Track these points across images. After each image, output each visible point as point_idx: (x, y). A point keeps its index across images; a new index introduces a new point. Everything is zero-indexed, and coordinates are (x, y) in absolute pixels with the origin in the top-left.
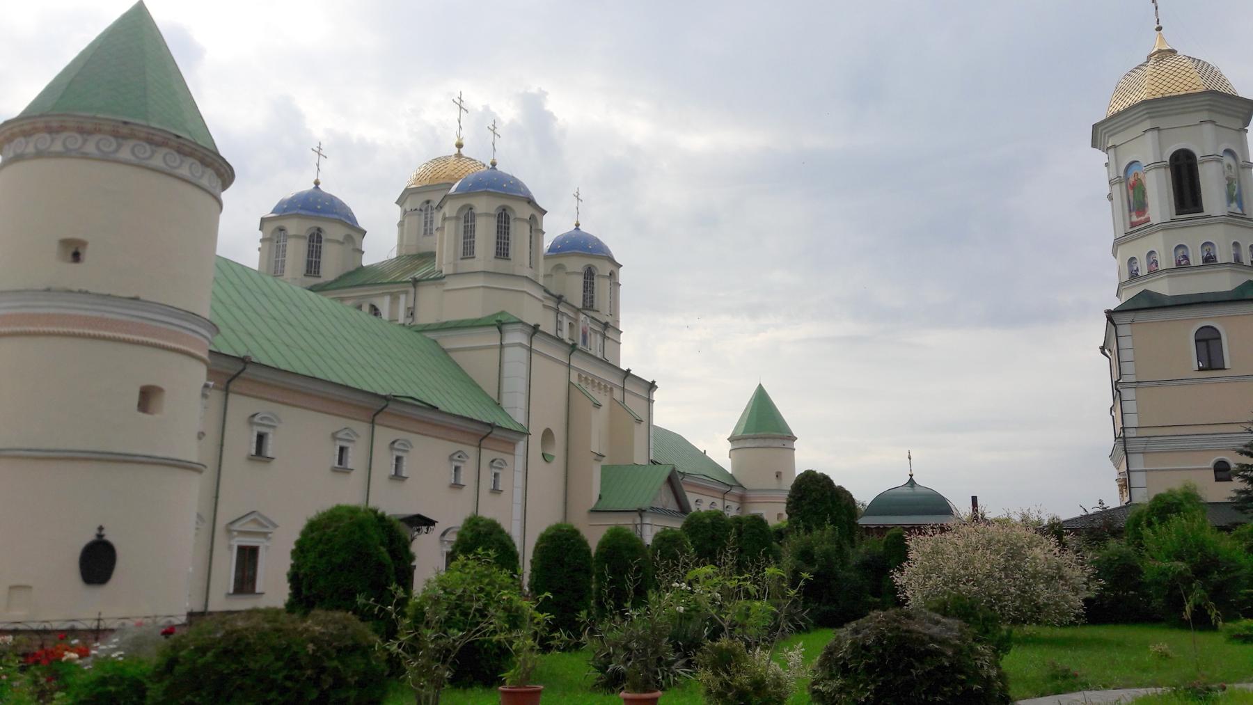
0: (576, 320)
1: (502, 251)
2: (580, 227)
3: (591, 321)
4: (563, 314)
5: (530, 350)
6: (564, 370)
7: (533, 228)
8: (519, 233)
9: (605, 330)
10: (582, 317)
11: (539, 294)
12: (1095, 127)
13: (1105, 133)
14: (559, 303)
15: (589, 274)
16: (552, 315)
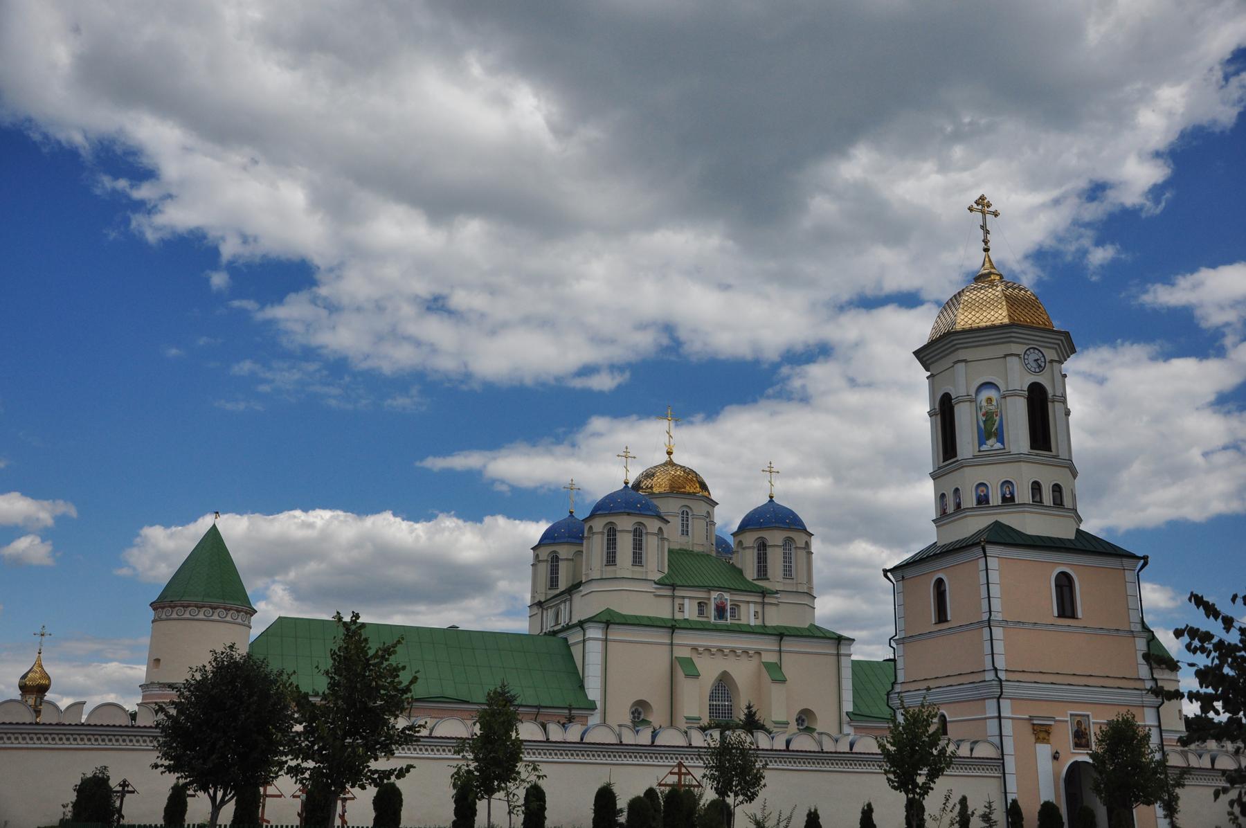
0: (709, 599)
1: (611, 560)
2: (773, 499)
3: (731, 594)
4: (683, 598)
5: (606, 640)
6: (668, 648)
7: (644, 531)
8: (625, 544)
9: (764, 598)
10: (714, 595)
11: (650, 587)
12: (1068, 332)
13: (1058, 344)
14: (674, 590)
15: (763, 546)
16: (668, 602)
